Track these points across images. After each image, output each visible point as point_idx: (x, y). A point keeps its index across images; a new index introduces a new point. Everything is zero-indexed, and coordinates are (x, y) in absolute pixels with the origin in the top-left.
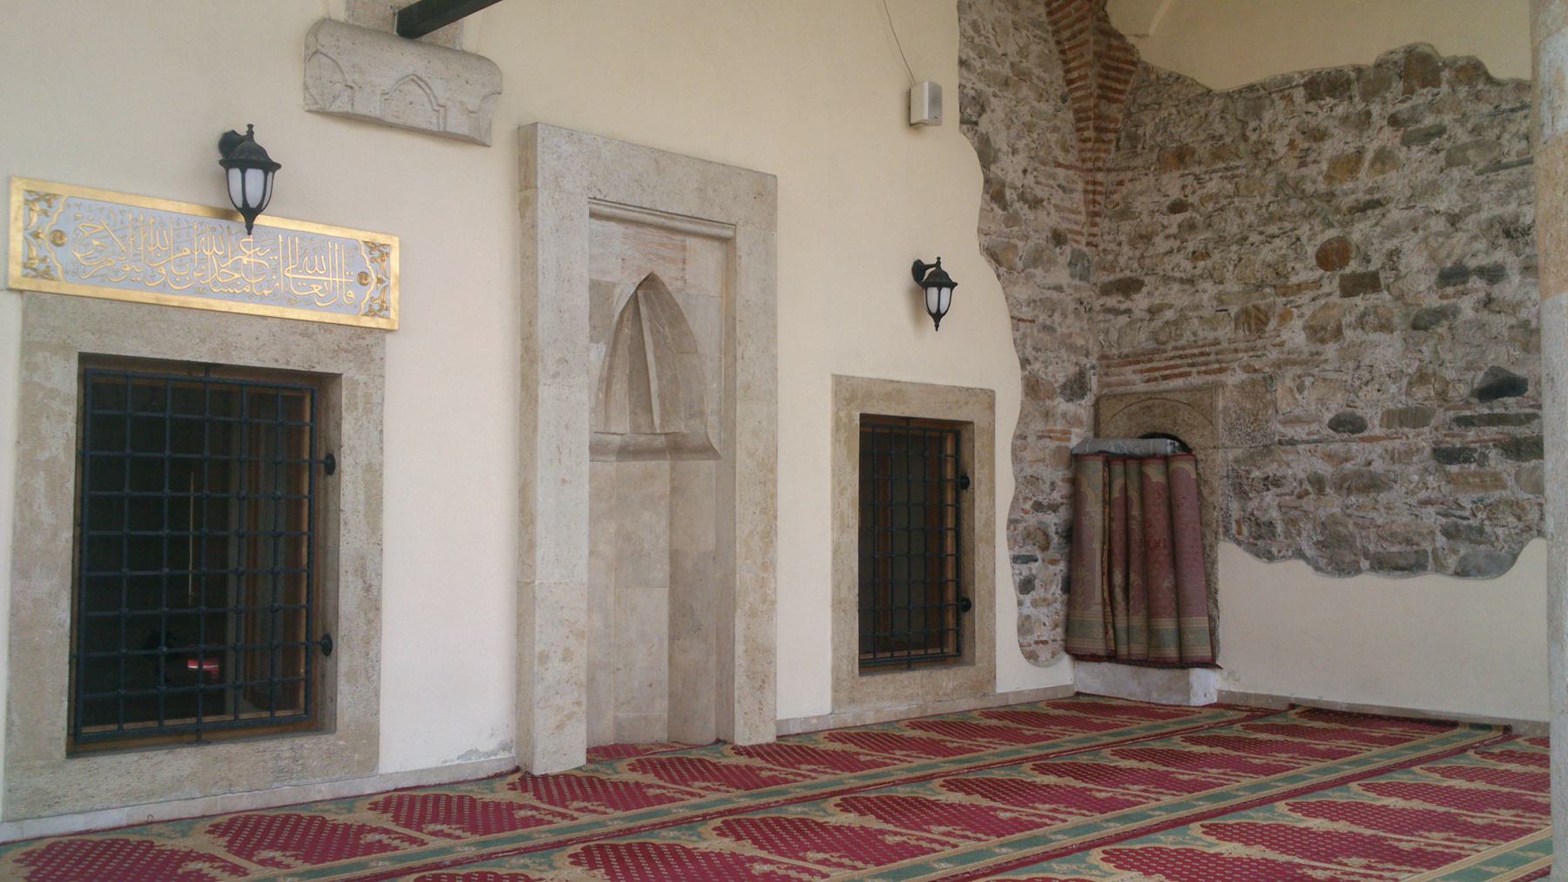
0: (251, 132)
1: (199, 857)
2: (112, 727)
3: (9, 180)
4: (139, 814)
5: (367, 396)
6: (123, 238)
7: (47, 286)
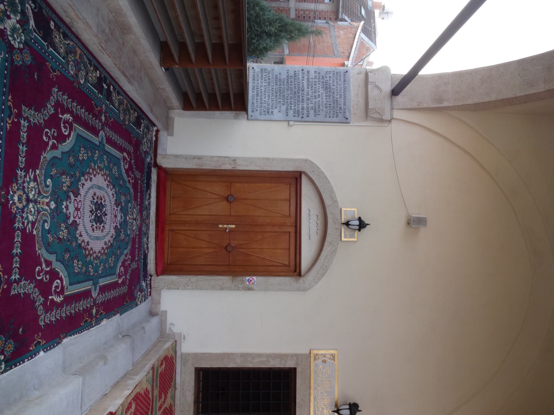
0: (359, 411)
1: (165, 399)
2: (201, 379)
3: (336, 350)
4: (178, 386)
6: (326, 378)
7: (312, 359)
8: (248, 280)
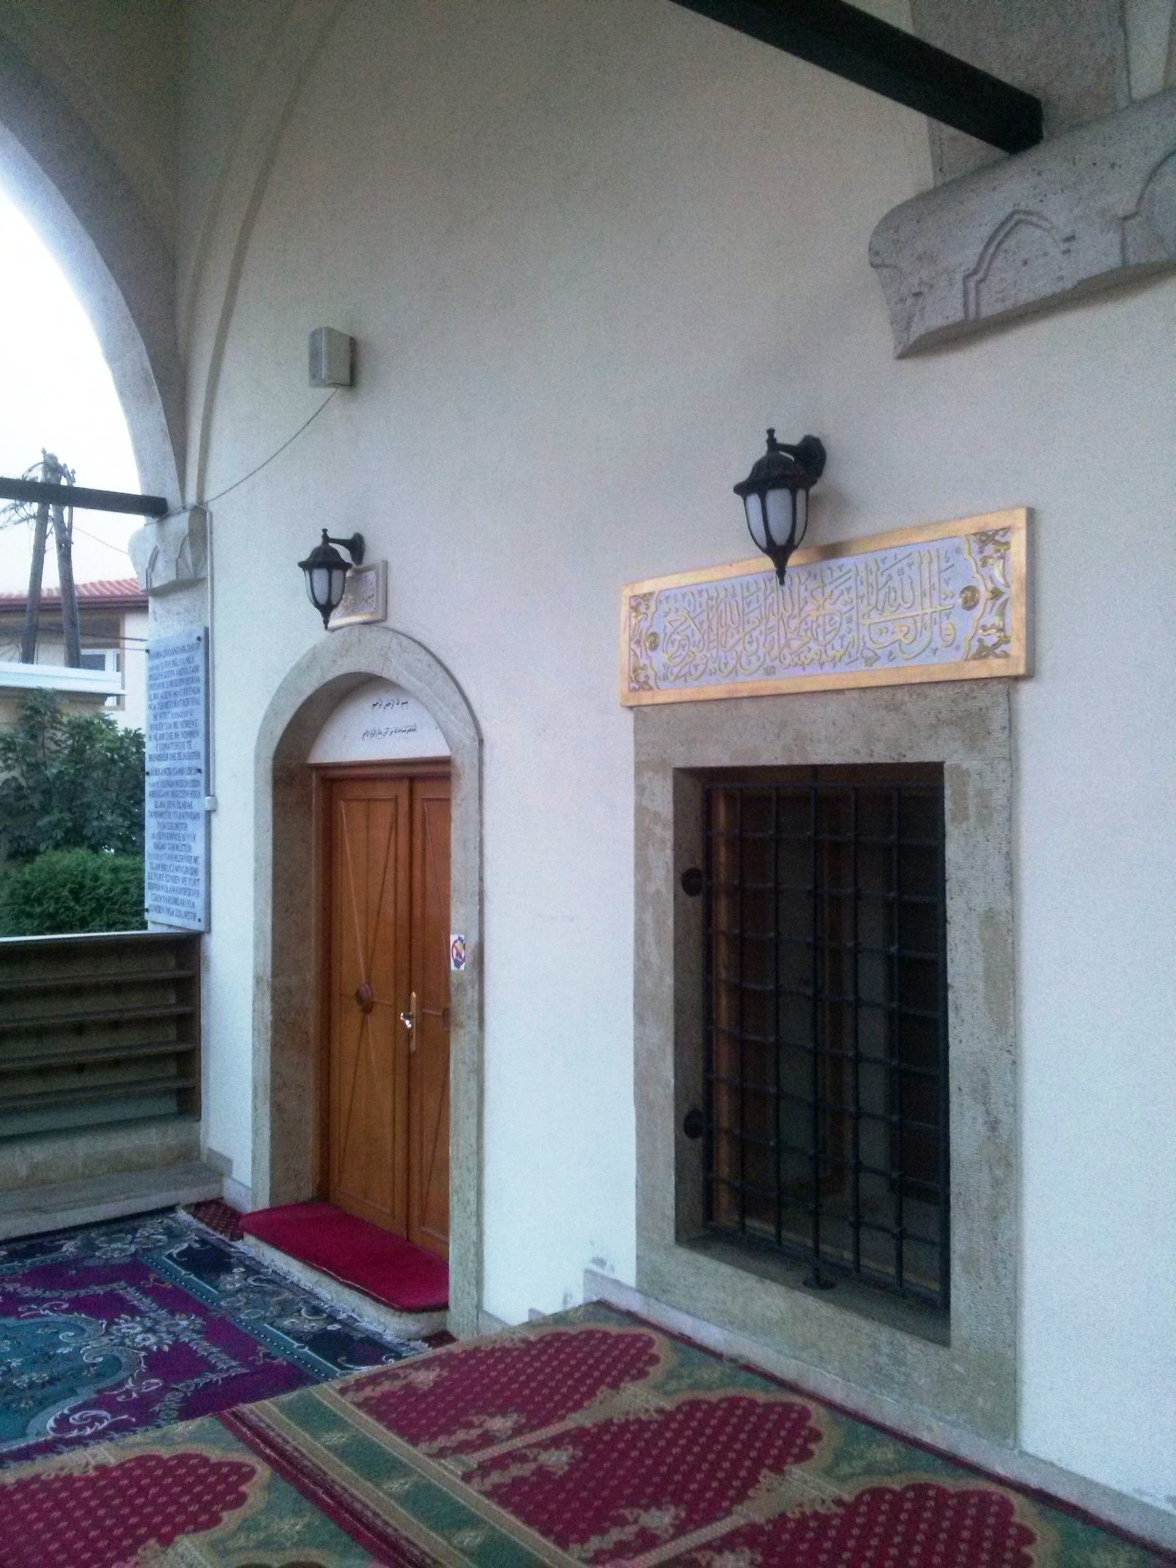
5: (984, 794)
7: (646, 698)
8: (458, 964)
